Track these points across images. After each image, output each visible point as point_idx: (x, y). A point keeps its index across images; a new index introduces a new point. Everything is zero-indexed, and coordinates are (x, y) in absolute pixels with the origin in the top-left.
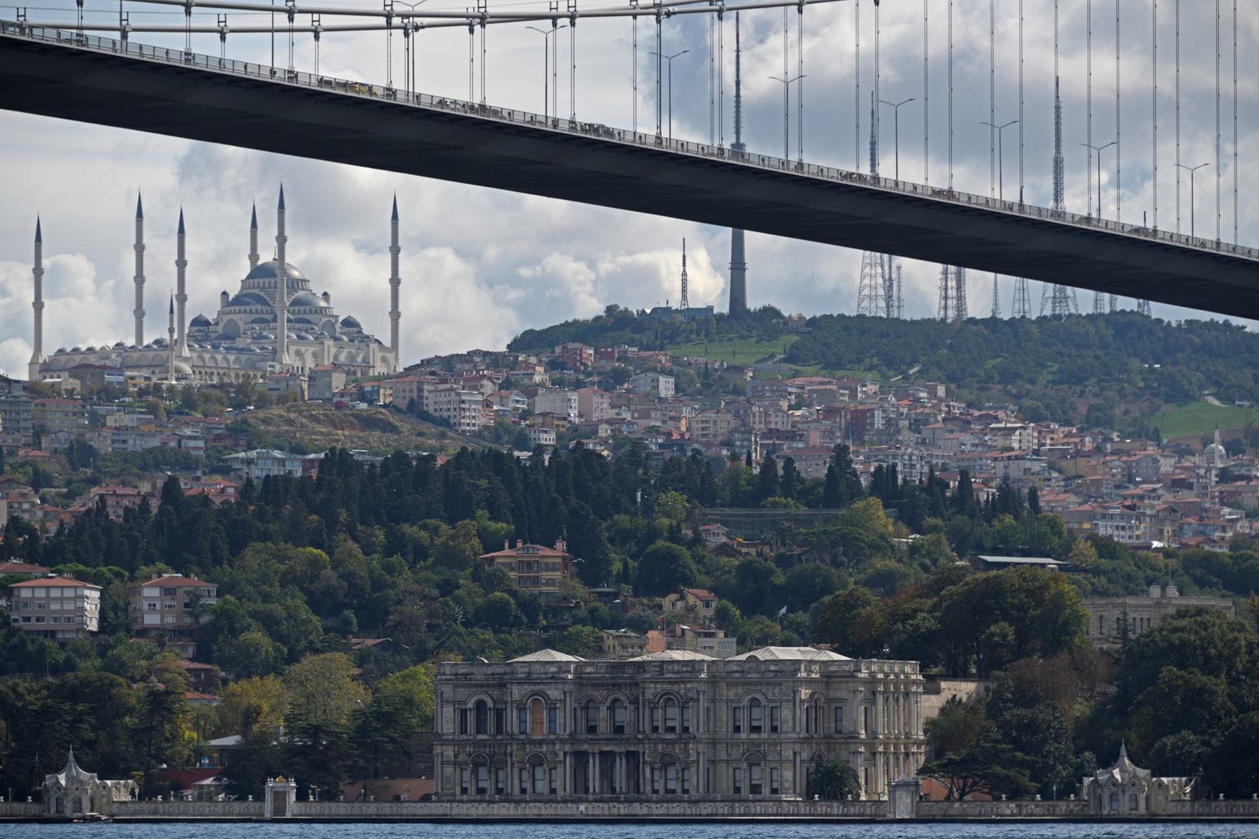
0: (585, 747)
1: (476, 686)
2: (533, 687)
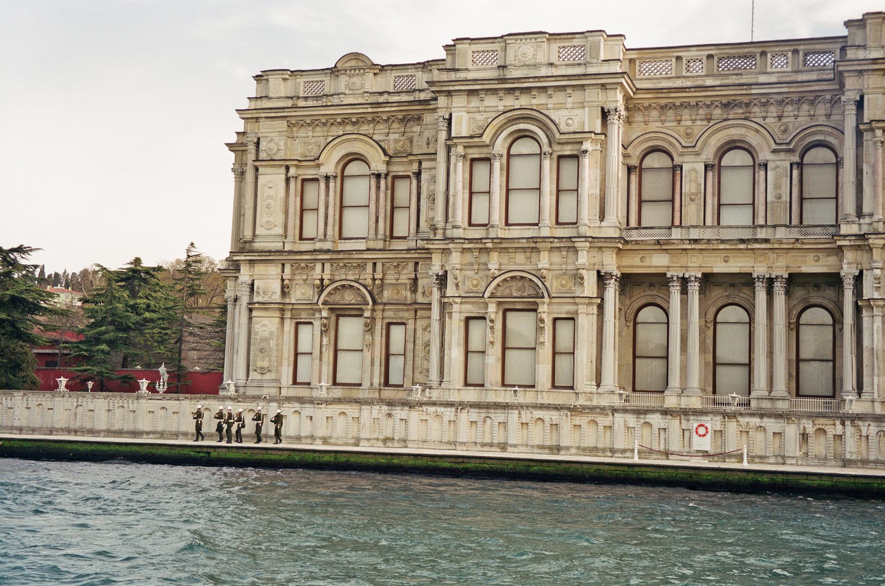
0: (658, 262)
2: (509, 102)
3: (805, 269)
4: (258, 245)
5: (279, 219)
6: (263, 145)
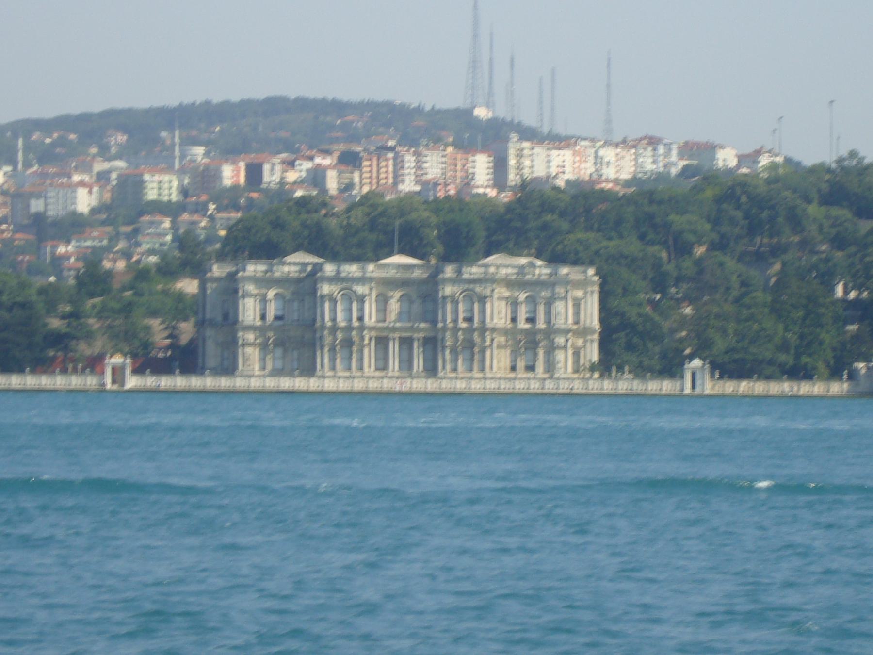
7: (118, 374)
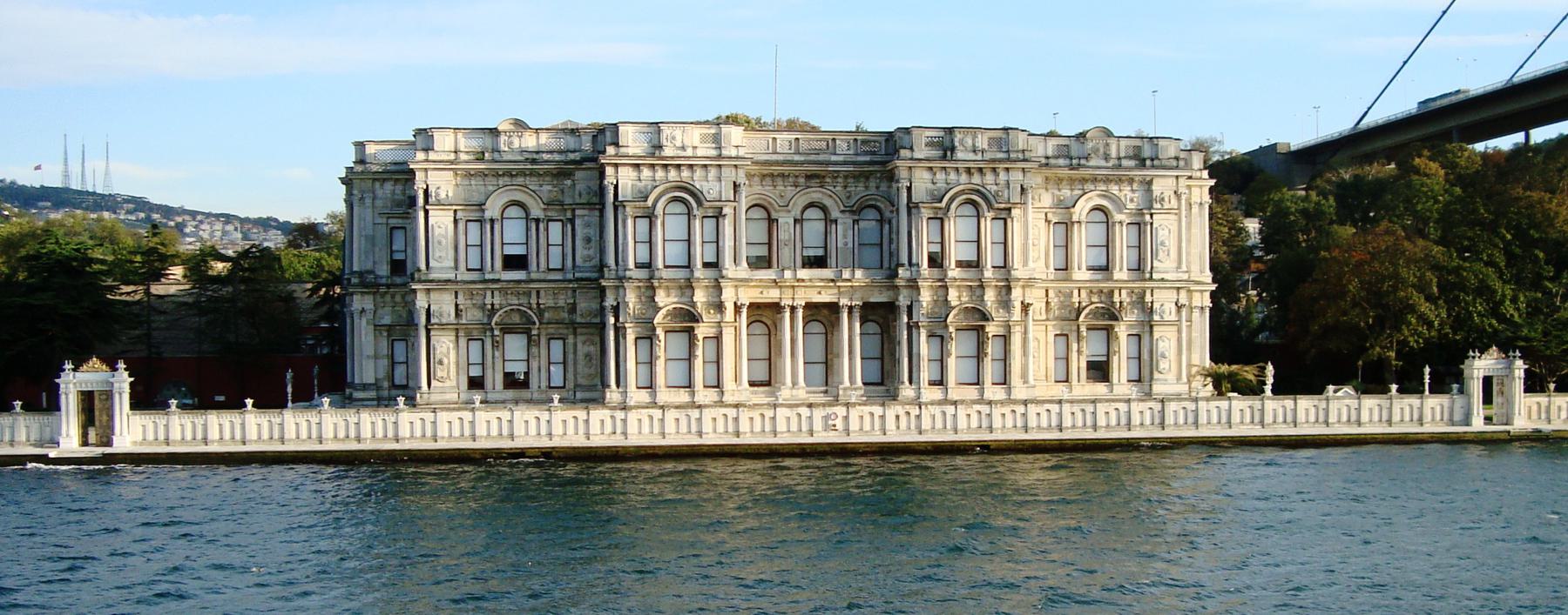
1: (509, 174)
3: (872, 300)
4: (433, 276)
5: (451, 252)
6: (432, 190)
7: (93, 409)
